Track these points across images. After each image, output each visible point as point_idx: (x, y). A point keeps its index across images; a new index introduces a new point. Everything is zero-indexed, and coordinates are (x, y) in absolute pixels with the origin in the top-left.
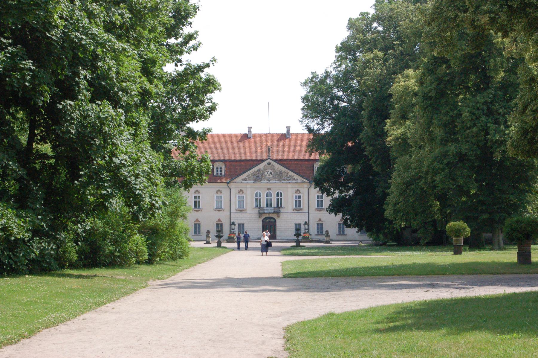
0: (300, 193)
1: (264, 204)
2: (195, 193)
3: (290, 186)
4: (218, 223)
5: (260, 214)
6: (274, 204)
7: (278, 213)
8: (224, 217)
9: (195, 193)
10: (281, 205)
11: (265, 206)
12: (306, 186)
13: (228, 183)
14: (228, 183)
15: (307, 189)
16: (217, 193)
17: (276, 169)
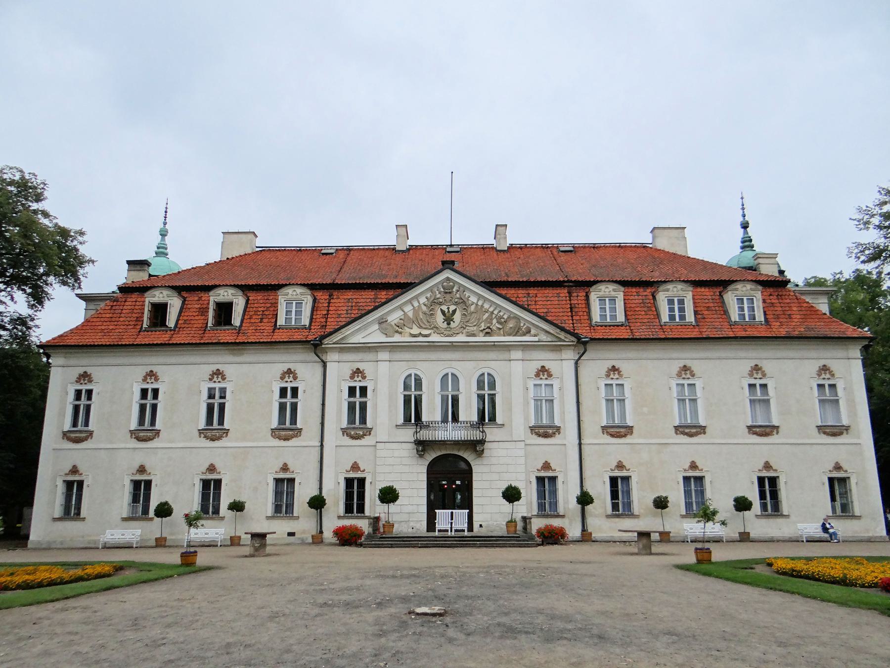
0: (550, 375)
1: (431, 411)
2: (210, 380)
3: (517, 354)
4: (282, 476)
5: (422, 446)
6: (469, 412)
7: (476, 446)
8: (299, 457)
9: (210, 380)
10: (493, 419)
11: (438, 418)
12: (570, 355)
13: (316, 346)
14: (316, 346)
15: (572, 364)
16: (282, 378)
17: (473, 299)
